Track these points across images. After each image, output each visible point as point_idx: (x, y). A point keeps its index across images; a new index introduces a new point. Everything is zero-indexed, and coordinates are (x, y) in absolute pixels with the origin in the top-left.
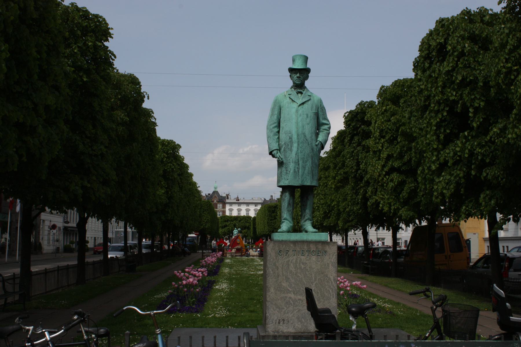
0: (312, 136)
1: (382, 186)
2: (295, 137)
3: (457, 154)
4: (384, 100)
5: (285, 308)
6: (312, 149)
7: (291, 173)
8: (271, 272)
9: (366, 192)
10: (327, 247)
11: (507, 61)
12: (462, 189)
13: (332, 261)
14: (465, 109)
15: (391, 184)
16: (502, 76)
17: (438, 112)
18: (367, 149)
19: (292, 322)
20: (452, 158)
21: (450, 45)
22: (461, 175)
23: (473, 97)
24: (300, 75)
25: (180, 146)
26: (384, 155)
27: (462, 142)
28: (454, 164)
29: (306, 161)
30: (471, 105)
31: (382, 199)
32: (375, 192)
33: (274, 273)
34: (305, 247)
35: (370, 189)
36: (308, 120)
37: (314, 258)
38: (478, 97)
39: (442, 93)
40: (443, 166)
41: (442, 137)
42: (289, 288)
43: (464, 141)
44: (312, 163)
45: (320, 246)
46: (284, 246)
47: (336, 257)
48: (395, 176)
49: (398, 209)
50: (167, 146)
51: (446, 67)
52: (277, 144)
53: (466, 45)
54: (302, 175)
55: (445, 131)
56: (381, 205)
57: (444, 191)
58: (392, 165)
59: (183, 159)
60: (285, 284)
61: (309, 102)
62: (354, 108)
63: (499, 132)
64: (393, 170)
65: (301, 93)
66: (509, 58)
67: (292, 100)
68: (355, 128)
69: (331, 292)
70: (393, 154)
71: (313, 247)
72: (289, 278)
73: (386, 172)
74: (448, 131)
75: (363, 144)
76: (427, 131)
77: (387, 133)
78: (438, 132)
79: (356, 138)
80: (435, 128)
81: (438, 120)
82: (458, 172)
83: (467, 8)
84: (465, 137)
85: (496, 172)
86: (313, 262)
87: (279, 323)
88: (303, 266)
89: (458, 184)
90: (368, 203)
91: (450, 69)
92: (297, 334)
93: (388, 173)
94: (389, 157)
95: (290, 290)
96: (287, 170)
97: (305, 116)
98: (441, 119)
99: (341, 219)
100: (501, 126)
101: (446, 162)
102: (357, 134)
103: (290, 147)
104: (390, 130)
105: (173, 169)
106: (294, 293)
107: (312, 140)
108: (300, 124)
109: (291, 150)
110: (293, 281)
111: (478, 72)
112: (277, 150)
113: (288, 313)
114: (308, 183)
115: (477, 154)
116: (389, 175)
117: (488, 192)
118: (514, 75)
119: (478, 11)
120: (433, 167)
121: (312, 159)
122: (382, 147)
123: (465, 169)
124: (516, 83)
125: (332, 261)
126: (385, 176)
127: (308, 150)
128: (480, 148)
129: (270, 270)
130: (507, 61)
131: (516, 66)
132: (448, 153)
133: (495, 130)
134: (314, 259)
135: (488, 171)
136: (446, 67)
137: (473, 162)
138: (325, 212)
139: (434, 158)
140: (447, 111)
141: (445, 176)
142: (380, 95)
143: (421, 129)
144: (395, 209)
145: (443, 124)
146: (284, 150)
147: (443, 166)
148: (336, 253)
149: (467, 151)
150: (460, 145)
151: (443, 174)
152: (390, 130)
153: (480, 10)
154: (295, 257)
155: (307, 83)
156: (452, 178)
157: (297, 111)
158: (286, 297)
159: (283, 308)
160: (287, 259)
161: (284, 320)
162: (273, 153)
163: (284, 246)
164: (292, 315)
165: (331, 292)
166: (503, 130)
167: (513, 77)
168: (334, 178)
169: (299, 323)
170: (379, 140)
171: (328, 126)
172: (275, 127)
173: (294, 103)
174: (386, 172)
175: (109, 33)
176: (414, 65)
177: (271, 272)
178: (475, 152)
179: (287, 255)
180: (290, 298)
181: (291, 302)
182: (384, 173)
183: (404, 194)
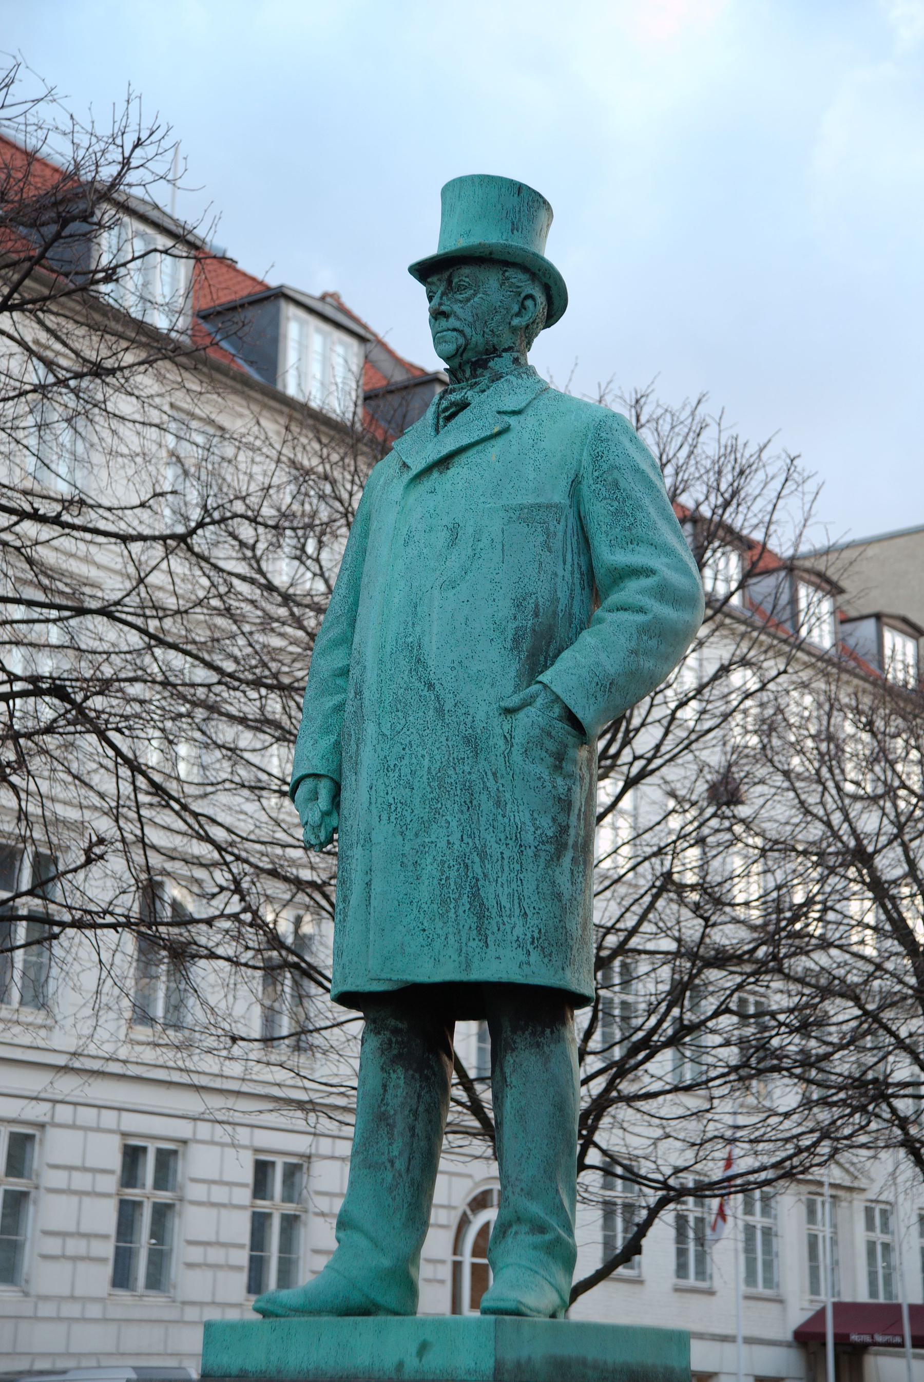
61: (494, 450)
97: (441, 538)
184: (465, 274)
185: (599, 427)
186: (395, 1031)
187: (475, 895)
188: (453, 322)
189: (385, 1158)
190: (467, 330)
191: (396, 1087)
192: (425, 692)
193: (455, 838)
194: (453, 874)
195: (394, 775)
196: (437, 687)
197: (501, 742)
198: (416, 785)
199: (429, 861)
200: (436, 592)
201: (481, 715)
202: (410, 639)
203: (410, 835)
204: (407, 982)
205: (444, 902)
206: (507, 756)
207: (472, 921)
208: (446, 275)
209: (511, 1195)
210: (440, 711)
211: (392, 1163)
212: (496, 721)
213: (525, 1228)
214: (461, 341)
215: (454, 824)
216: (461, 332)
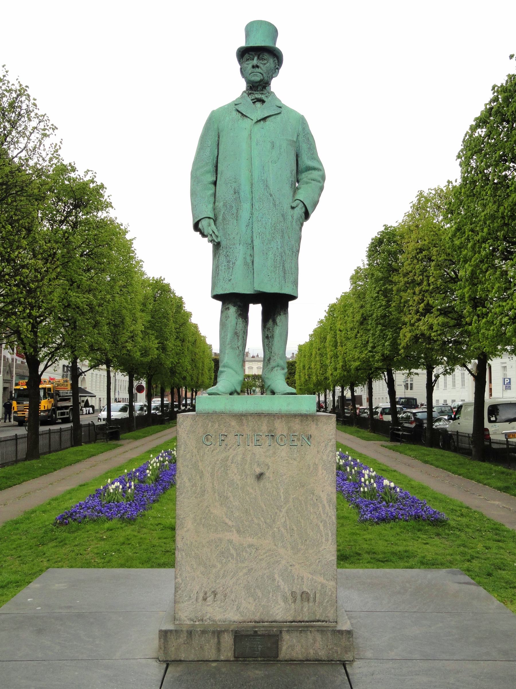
5: (219, 566)
8: (188, 484)
13: (325, 457)
19: (233, 597)
33: (194, 485)
37: (283, 451)
42: (227, 521)
45: (296, 425)
46: (216, 426)
52: (211, 206)
60: (218, 511)
65: (263, 101)
67: (242, 114)
69: (322, 528)
71: (280, 427)
72: (227, 498)
86: (281, 460)
87: (205, 599)
92: (245, 624)
95: (230, 523)
96: (228, 262)
97: (269, 146)
106: (238, 531)
109: (237, 217)
110: (237, 503)
112: (209, 218)
113: (224, 576)
125: (325, 457)
129: (186, 479)
134: (283, 454)
146: (224, 219)
154: (241, 449)
155: (276, 85)
158: (220, 540)
159: (214, 566)
160: (224, 455)
161: (215, 594)
162: (200, 226)
163: (216, 426)
164: (234, 580)
165: (322, 528)
169: (251, 600)
171: (320, 173)
172: (208, 172)
173: (246, 119)
177: (188, 484)
180: (230, 542)
181: (233, 551)
184: (266, 56)
186: (239, 306)
187: (283, 266)
188: (259, 70)
189: (236, 346)
190: (264, 75)
191: (240, 324)
192: (269, 197)
193: (279, 247)
194: (278, 258)
196: (273, 196)
197: (290, 218)
198: (267, 228)
199: (271, 253)
200: (270, 164)
201: (285, 208)
202: (263, 178)
203: (265, 244)
204: (259, 291)
205: (275, 267)
206: (292, 222)
207: (282, 274)
208: (259, 53)
209: (276, 359)
210: (275, 205)
211: (238, 347)
213: (279, 368)
214: (262, 78)
215: (279, 242)
216: (262, 74)
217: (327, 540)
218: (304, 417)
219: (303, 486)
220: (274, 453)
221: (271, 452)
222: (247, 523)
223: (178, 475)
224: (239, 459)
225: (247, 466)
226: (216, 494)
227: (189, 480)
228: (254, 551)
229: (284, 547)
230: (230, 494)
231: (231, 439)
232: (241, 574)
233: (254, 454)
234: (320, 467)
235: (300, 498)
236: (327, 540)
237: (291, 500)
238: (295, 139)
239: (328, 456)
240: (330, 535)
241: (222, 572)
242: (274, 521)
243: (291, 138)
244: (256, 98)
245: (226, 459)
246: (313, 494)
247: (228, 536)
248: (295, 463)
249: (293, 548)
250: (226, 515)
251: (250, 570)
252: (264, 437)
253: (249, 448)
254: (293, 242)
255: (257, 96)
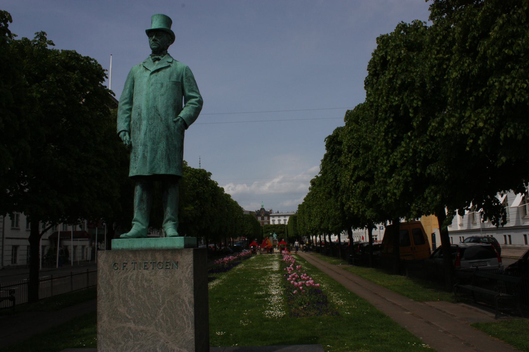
0: (167, 110)
1: (352, 193)
2: (144, 112)
3: (404, 155)
4: (349, 121)
5: (123, 343)
6: (168, 127)
7: (139, 160)
8: (104, 294)
9: (342, 199)
10: (179, 257)
11: (438, 53)
12: (411, 188)
13: (187, 275)
14: (407, 112)
15: (358, 190)
16: (435, 69)
17: (386, 119)
18: (340, 163)
20: (400, 159)
21: (390, 55)
22: (408, 174)
23: (412, 98)
24: (162, 39)
25: (210, 174)
26: (351, 167)
27: (406, 143)
28: (402, 165)
29: (158, 143)
30: (411, 107)
31: (353, 203)
32: (348, 199)
34: (149, 258)
35: (345, 196)
36: (163, 90)
37: (161, 273)
38: (416, 97)
39: (387, 101)
40: (393, 168)
41: (390, 141)
42: (128, 316)
43: (408, 141)
44: (167, 144)
45: (169, 256)
46: (121, 258)
47: (192, 270)
48: (361, 184)
49: (365, 211)
50: (199, 173)
51: (388, 75)
52: (127, 123)
53: (402, 52)
54: (152, 162)
55: (392, 135)
56: (352, 209)
57: (395, 191)
58: (358, 175)
59: (217, 184)
60: (122, 310)
61: (168, 69)
62: (331, 133)
63: (437, 125)
64: (359, 179)
66: (441, 49)
68: (333, 149)
69: (185, 319)
70: (358, 165)
71: (159, 258)
72: (127, 302)
73: (354, 181)
74: (395, 136)
75: (339, 160)
76: (378, 139)
77: (353, 148)
78: (387, 137)
79: (334, 158)
80: (383, 134)
81: (385, 126)
82: (405, 171)
83: (402, 22)
84: (409, 138)
85: (439, 167)
86: (160, 278)
88: (146, 284)
89: (406, 184)
90: (345, 208)
91: (391, 76)
93: (355, 182)
94: (355, 168)
95: (129, 317)
96: (135, 156)
97: (159, 86)
98: (388, 126)
99: (331, 222)
100: (437, 119)
101: (395, 163)
102: (334, 154)
103: (138, 125)
104: (355, 145)
105: (204, 191)
106: (134, 322)
107: (168, 115)
108: (151, 96)
109: (140, 130)
110: (133, 305)
111: (415, 74)
114: (162, 171)
115: (420, 152)
116: (356, 183)
117: (433, 187)
118: (446, 64)
119: (413, 24)
120: (385, 170)
121: (167, 140)
122: (350, 160)
123: (411, 168)
124: (448, 71)
125: (187, 275)
126: (353, 184)
127: (161, 128)
128: (422, 146)
129: (103, 290)
130: (438, 53)
131: (447, 54)
132: (396, 154)
133: (433, 124)
134: (161, 274)
135: (431, 168)
136: (388, 75)
137: (418, 160)
138: (322, 218)
139: (385, 162)
140: (393, 118)
141: (396, 177)
142: (346, 118)
143: (374, 139)
144: (362, 212)
145: (391, 130)
146: (133, 131)
147: (393, 168)
148: (192, 265)
149: (411, 150)
150: (404, 145)
151: (394, 175)
152: (355, 145)
153: (415, 24)
154: (135, 272)
156: (401, 178)
157: (150, 79)
158: (124, 327)
159: (120, 344)
160: (125, 275)
163: (121, 258)
165: (185, 319)
166: (441, 123)
167: (445, 66)
168: (324, 191)
170: (348, 155)
172: (126, 103)
174: (354, 181)
175: (105, 75)
176: (365, 84)
177: (104, 294)
178: (418, 150)
179: (125, 269)
180: (130, 328)
181: (131, 334)
182: (352, 182)
183: (369, 197)
185: (186, 68)
187: (168, 158)
193: (165, 146)
194: (164, 153)
195: (152, 132)
205: (162, 158)
212: (172, 123)
217: (189, 327)
218: (174, 251)
219: (173, 294)
220: (156, 273)
221: (153, 273)
222: (140, 317)
223: (98, 288)
224: (134, 277)
225: (139, 282)
226: (121, 300)
227: (105, 291)
228: (144, 334)
229: (162, 331)
230: (129, 299)
231: (129, 266)
232: (136, 348)
233: (143, 274)
234: (184, 282)
235: (172, 301)
236: (189, 327)
237: (166, 302)
238: (180, 81)
239: (189, 274)
240: (190, 323)
241: (125, 347)
242: (156, 315)
243: (175, 80)
244: (155, 58)
245: (126, 278)
246: (180, 298)
247: (129, 325)
248: (168, 279)
249: (167, 332)
250: (127, 312)
251: (142, 346)
252: (149, 263)
253: (140, 271)
254: (176, 143)
255: (156, 57)
